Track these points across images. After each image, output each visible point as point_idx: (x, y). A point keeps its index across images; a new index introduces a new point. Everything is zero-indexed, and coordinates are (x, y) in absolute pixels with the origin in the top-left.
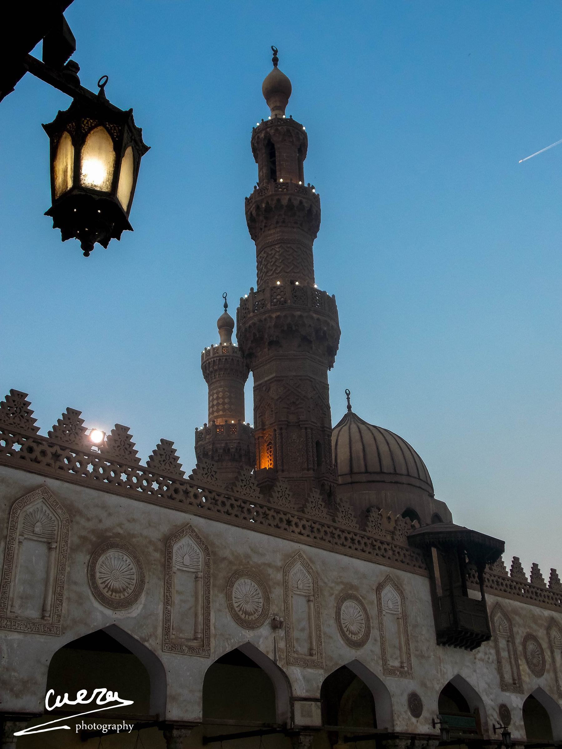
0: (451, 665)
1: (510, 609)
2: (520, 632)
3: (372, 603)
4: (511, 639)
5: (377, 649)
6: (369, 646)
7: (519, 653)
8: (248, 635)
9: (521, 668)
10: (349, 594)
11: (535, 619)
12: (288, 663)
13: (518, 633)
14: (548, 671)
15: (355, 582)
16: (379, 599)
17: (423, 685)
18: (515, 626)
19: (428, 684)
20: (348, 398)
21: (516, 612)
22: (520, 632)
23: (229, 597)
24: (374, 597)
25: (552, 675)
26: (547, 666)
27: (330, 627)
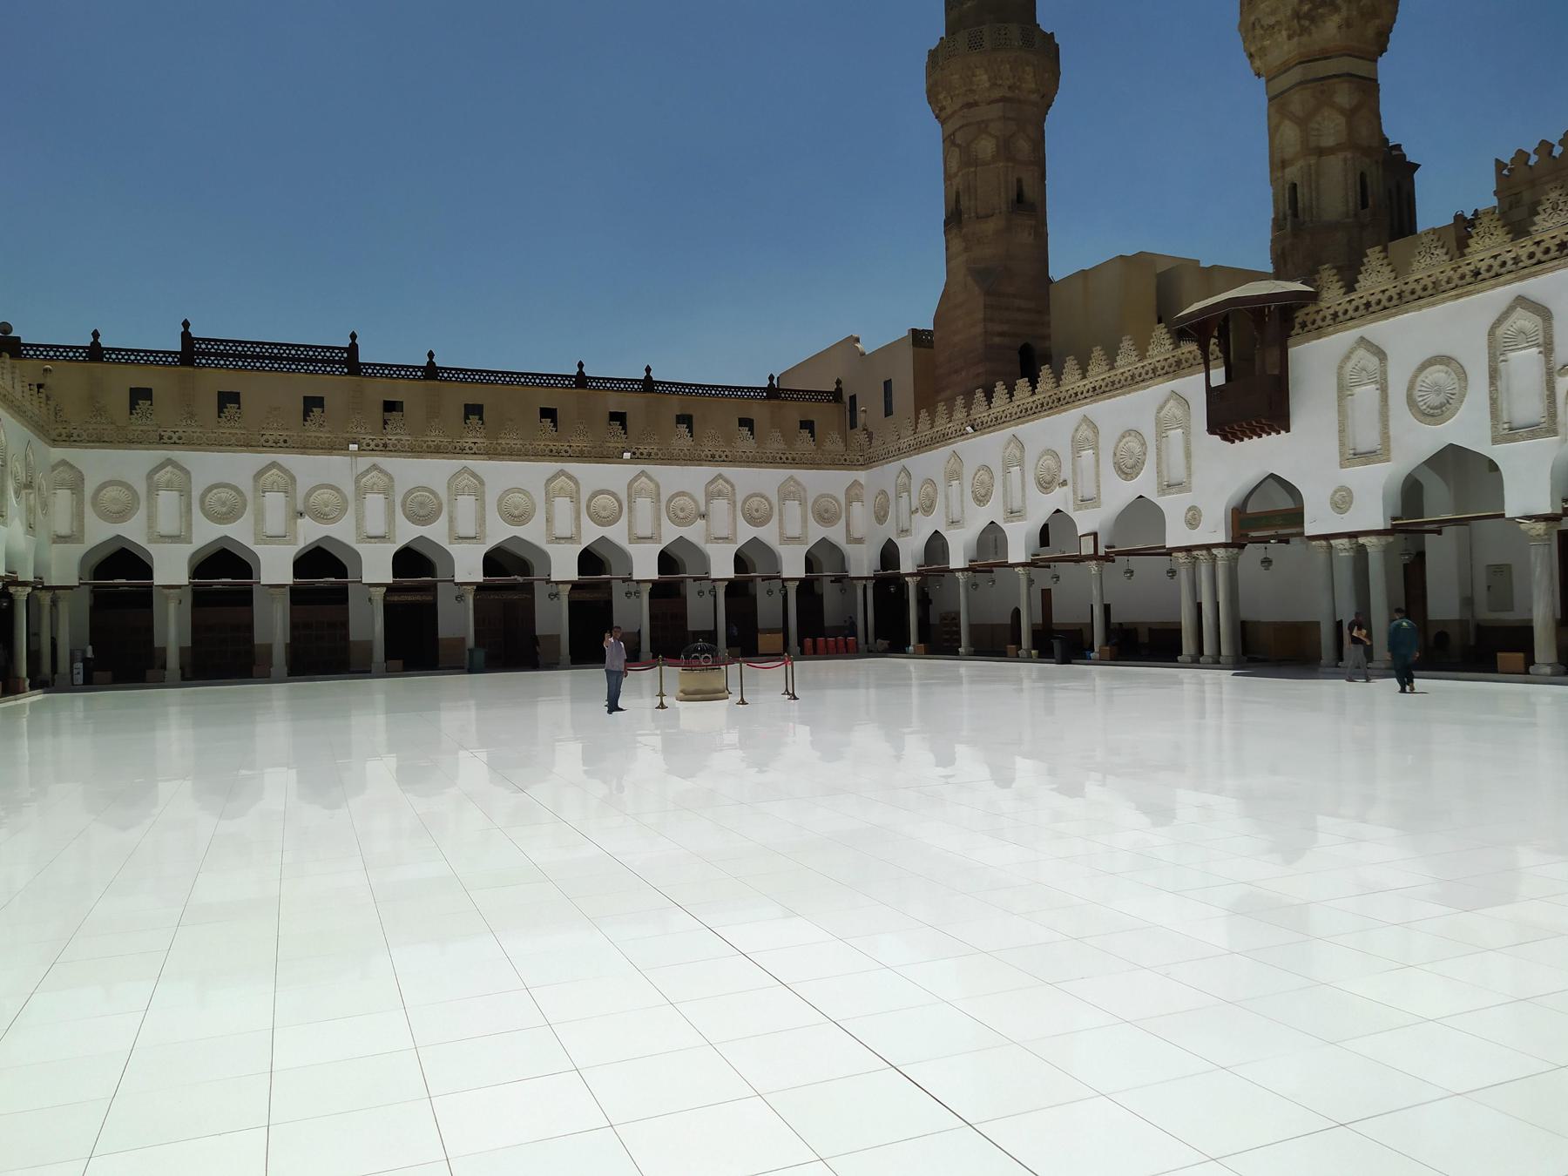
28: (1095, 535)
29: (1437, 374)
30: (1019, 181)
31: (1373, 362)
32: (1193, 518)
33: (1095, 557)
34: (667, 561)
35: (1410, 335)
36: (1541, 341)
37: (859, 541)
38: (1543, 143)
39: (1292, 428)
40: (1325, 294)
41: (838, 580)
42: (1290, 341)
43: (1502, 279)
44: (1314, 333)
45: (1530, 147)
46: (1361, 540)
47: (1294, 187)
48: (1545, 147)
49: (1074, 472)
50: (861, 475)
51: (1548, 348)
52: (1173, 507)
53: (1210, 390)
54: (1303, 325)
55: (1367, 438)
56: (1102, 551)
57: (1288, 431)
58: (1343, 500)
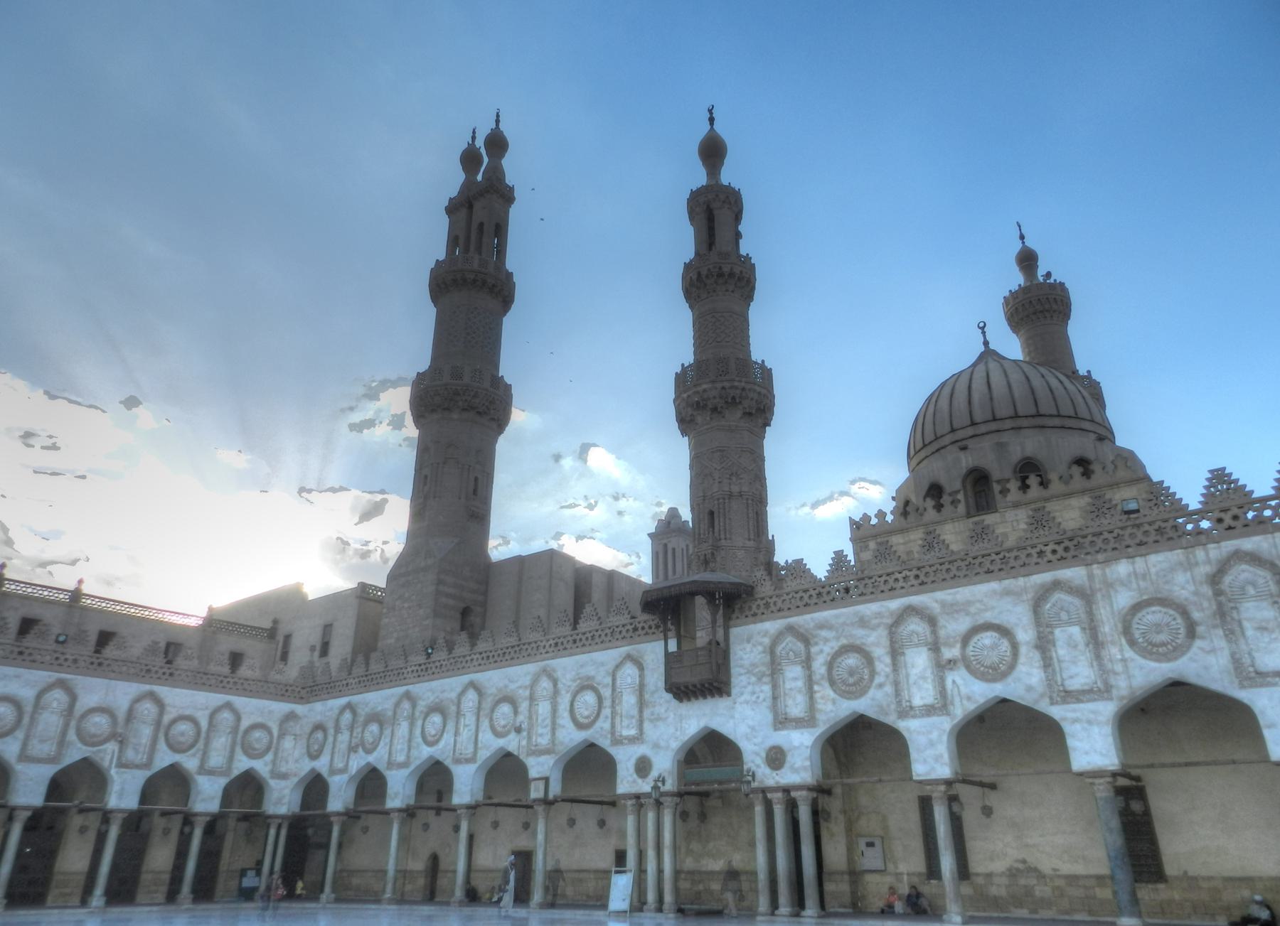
0: (695, 718)
1: (812, 625)
2: (822, 653)
3: (606, 686)
4: (807, 663)
5: (607, 726)
6: (599, 724)
7: (816, 677)
8: (501, 742)
9: (818, 695)
10: (587, 685)
11: (863, 622)
12: (528, 755)
13: (821, 651)
14: (881, 686)
15: (592, 673)
16: (614, 680)
17: (656, 746)
18: (816, 644)
19: (662, 744)
20: (984, 333)
21: (821, 626)
22: (822, 653)
23: (491, 720)
24: (609, 680)
25: (889, 689)
26: (878, 680)
27: (564, 718)
28: (547, 780)
29: (852, 660)
30: (476, 479)
31: (800, 646)
32: (643, 767)
33: (547, 802)
34: (57, 787)
35: (832, 625)
36: (930, 640)
37: (284, 776)
38: (880, 511)
39: (734, 691)
40: (759, 589)
41: (245, 818)
42: (732, 623)
43: (896, 592)
44: (750, 619)
45: (872, 513)
46: (793, 794)
47: (712, 513)
48: (881, 514)
49: (530, 718)
50: (299, 709)
51: (935, 648)
52: (625, 758)
53: (667, 655)
54: (741, 609)
55: (796, 707)
56: (551, 796)
57: (729, 694)
58: (776, 758)
